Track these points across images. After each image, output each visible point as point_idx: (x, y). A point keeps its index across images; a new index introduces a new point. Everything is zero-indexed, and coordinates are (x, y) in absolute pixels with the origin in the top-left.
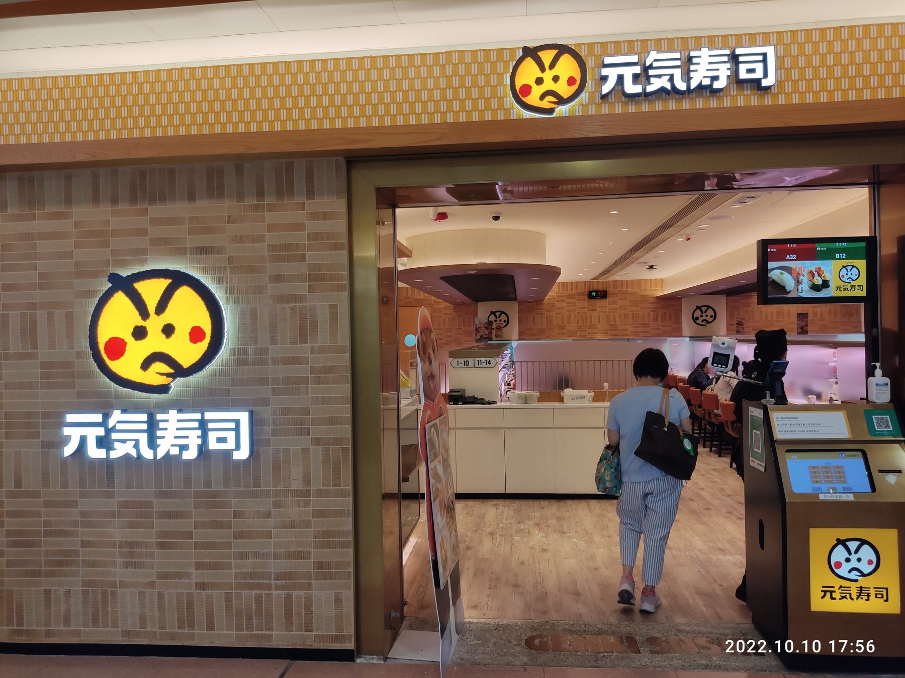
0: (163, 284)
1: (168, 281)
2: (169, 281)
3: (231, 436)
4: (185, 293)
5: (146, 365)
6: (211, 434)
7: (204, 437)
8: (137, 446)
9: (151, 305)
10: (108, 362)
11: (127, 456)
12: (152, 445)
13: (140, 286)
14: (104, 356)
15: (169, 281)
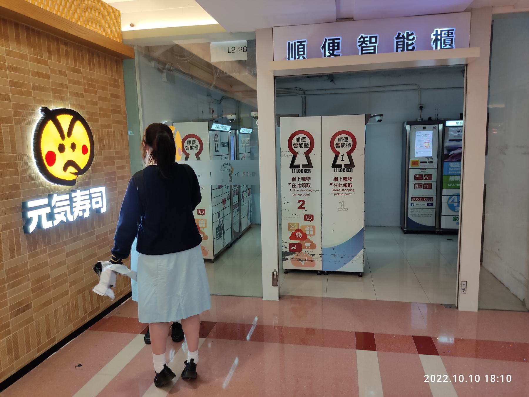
3: (99, 199)
7: (91, 203)
8: (65, 215)
9: (65, 130)
10: (48, 167)
11: (62, 222)
12: (72, 213)
14: (46, 163)
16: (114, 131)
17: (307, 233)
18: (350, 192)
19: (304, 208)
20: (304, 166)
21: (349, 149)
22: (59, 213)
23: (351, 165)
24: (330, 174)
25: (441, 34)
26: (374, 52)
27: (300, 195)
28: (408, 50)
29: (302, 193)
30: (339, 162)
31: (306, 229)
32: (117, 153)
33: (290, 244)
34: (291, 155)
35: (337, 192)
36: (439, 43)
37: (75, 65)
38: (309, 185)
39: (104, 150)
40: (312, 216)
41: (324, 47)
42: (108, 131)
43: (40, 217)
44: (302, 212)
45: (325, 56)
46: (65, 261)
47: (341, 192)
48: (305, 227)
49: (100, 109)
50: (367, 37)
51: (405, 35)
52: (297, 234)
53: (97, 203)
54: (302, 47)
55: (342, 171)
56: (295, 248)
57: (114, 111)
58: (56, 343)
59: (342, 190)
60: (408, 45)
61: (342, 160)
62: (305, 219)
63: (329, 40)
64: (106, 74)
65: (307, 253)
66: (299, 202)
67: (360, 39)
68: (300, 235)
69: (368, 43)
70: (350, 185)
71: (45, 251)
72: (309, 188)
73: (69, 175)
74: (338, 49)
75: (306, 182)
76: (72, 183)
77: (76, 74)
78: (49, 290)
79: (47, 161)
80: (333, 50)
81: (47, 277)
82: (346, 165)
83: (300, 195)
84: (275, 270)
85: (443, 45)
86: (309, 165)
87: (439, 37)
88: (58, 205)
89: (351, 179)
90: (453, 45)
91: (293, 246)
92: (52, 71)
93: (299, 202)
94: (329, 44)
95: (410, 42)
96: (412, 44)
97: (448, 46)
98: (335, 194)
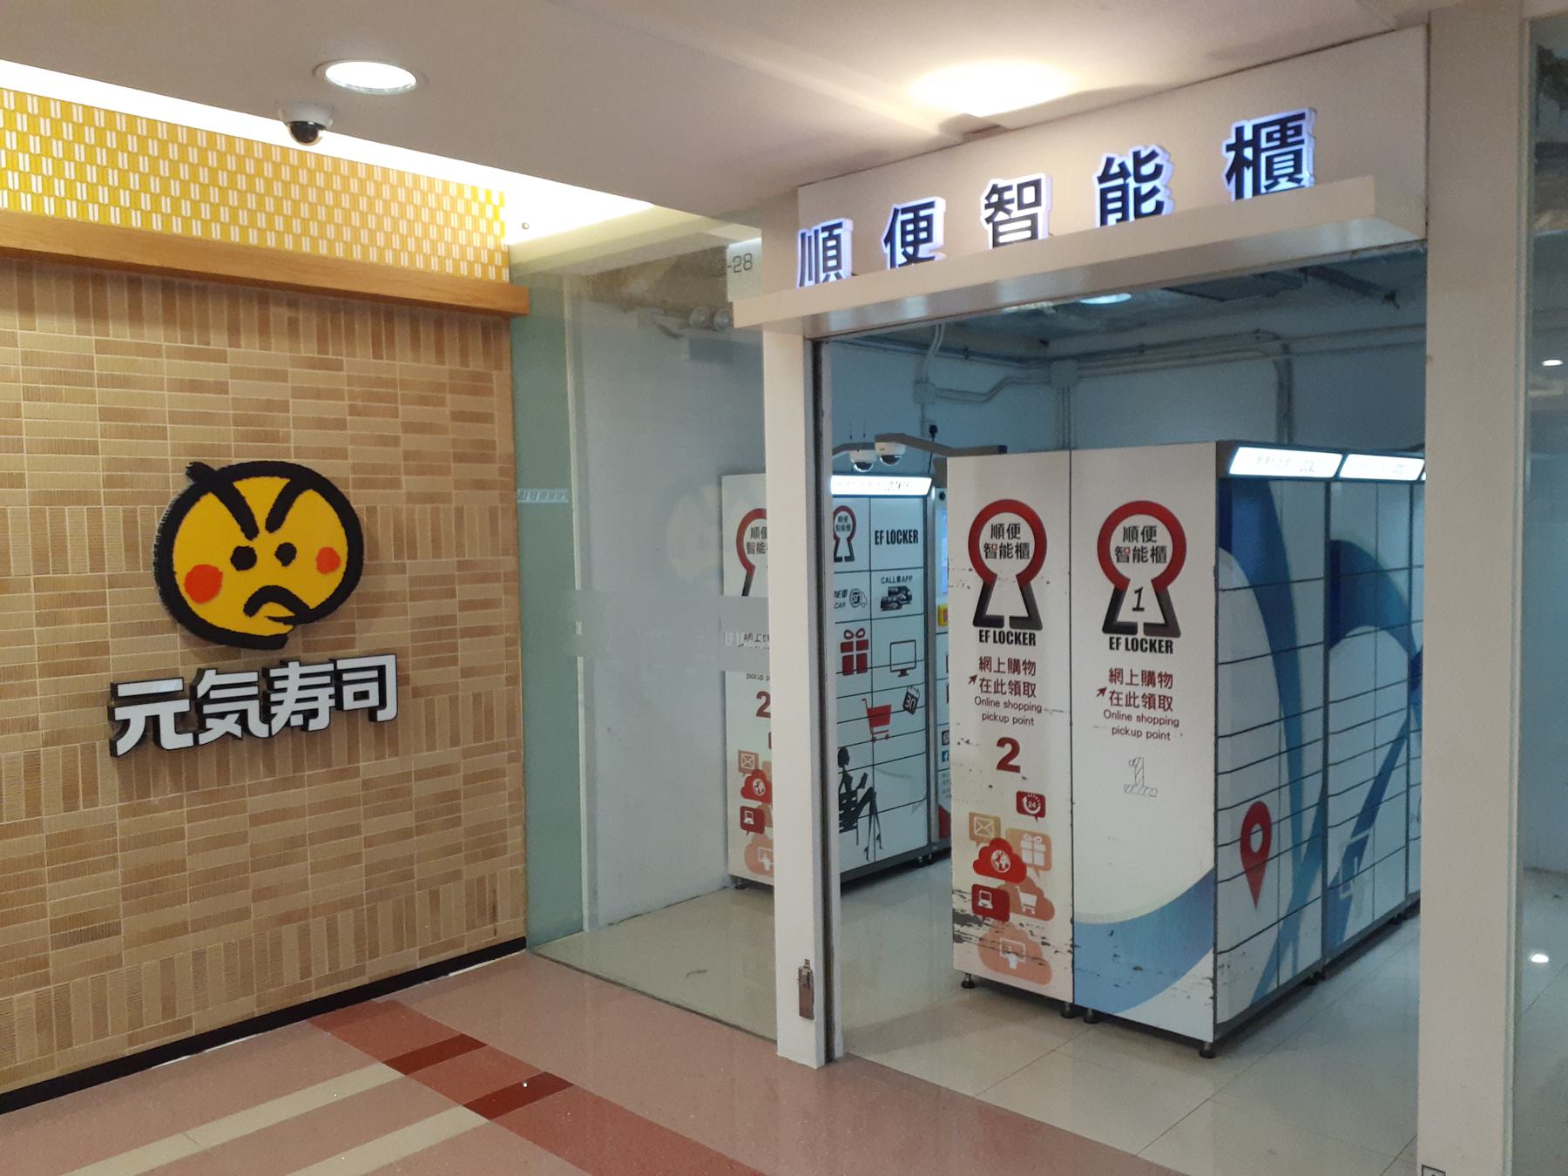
0: (277, 484)
1: (284, 482)
2: (285, 481)
3: (373, 688)
4: (310, 503)
5: (251, 607)
6: (346, 688)
7: (338, 696)
8: (243, 717)
12: (266, 717)
13: (244, 487)
15: (285, 481)
16: (459, 512)
17: (1026, 858)
18: (1165, 729)
19: (1016, 769)
20: (1015, 621)
21: (1160, 568)
22: (222, 715)
23: (1168, 628)
24: (1098, 655)
25: (1255, 143)
26: (1034, 236)
27: (1004, 720)
28: (1138, 214)
29: (1011, 713)
30: (1125, 615)
31: (1023, 844)
32: (462, 565)
33: (976, 888)
34: (977, 583)
35: (1122, 724)
36: (1248, 174)
37: (322, 349)
38: (1029, 689)
39: (413, 556)
40: (1042, 799)
41: (890, 239)
42: (435, 512)
43: (153, 723)
44: (1011, 784)
45: (893, 264)
46: (246, 835)
47: (1133, 725)
48: (1019, 834)
49: (407, 455)
50: (1009, 188)
51: (1130, 167)
52: (994, 856)
53: (364, 695)
54: (832, 243)
55: (1135, 646)
56: (990, 906)
57: (460, 458)
58: (192, 1033)
59: (1140, 719)
60: (1140, 199)
61: (1138, 609)
62: (1020, 809)
63: (905, 211)
64: (441, 361)
65: (1026, 929)
66: (1002, 743)
67: (988, 198)
68: (1005, 860)
69: (1013, 207)
70: (1166, 702)
71: (174, 804)
72: (1032, 701)
73: (263, 624)
74: (929, 239)
75: (1022, 677)
76: (278, 642)
77: (320, 372)
78: (181, 900)
79: (188, 590)
80: (916, 243)
81: (181, 866)
82: (1150, 628)
83: (1004, 720)
84: (807, 962)
85: (1264, 182)
86: (1031, 621)
87: (1248, 153)
88: (214, 695)
89: (1167, 678)
90: (1306, 175)
91: (985, 897)
92: (236, 373)
93: (1002, 743)
94: (904, 223)
95: (1146, 188)
96: (1154, 191)
97: (1284, 184)
98: (1115, 731)
